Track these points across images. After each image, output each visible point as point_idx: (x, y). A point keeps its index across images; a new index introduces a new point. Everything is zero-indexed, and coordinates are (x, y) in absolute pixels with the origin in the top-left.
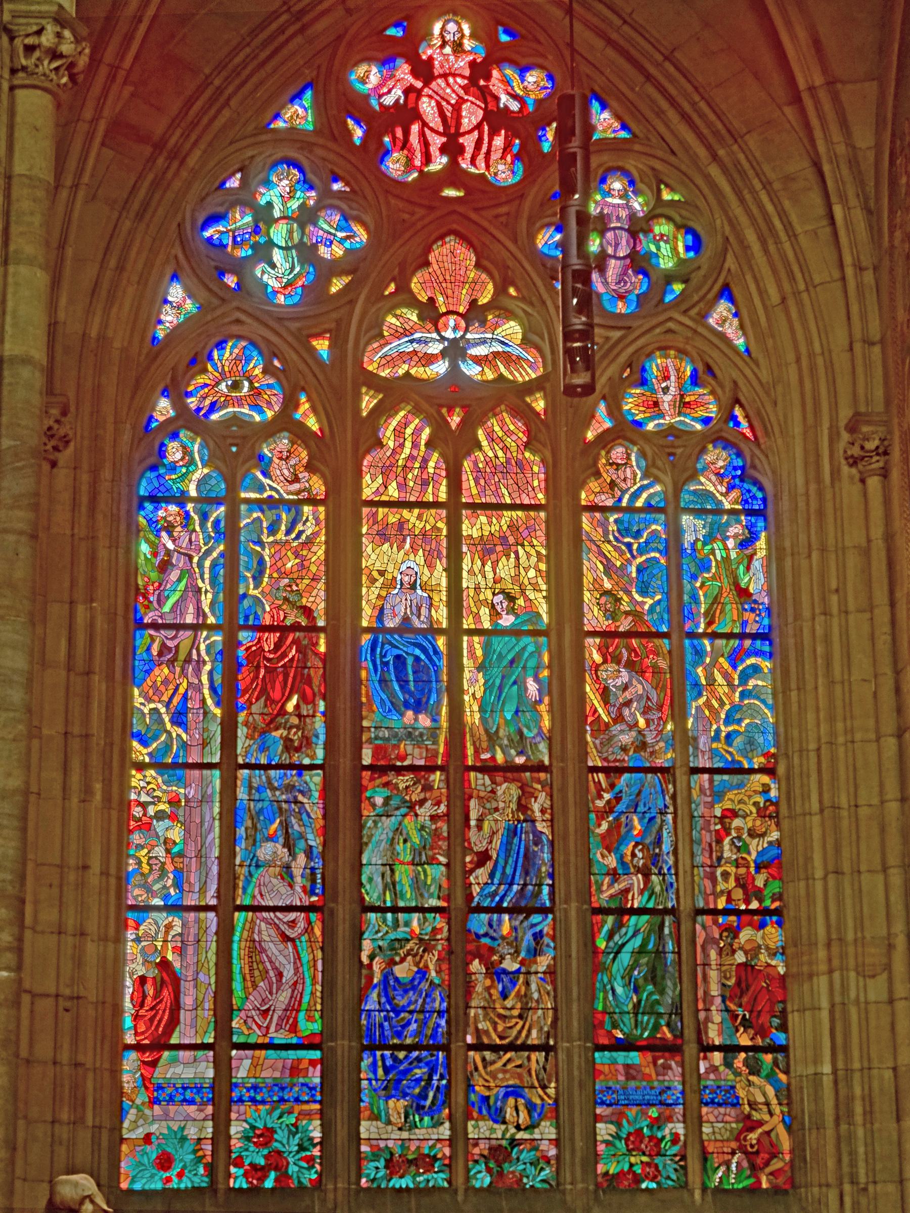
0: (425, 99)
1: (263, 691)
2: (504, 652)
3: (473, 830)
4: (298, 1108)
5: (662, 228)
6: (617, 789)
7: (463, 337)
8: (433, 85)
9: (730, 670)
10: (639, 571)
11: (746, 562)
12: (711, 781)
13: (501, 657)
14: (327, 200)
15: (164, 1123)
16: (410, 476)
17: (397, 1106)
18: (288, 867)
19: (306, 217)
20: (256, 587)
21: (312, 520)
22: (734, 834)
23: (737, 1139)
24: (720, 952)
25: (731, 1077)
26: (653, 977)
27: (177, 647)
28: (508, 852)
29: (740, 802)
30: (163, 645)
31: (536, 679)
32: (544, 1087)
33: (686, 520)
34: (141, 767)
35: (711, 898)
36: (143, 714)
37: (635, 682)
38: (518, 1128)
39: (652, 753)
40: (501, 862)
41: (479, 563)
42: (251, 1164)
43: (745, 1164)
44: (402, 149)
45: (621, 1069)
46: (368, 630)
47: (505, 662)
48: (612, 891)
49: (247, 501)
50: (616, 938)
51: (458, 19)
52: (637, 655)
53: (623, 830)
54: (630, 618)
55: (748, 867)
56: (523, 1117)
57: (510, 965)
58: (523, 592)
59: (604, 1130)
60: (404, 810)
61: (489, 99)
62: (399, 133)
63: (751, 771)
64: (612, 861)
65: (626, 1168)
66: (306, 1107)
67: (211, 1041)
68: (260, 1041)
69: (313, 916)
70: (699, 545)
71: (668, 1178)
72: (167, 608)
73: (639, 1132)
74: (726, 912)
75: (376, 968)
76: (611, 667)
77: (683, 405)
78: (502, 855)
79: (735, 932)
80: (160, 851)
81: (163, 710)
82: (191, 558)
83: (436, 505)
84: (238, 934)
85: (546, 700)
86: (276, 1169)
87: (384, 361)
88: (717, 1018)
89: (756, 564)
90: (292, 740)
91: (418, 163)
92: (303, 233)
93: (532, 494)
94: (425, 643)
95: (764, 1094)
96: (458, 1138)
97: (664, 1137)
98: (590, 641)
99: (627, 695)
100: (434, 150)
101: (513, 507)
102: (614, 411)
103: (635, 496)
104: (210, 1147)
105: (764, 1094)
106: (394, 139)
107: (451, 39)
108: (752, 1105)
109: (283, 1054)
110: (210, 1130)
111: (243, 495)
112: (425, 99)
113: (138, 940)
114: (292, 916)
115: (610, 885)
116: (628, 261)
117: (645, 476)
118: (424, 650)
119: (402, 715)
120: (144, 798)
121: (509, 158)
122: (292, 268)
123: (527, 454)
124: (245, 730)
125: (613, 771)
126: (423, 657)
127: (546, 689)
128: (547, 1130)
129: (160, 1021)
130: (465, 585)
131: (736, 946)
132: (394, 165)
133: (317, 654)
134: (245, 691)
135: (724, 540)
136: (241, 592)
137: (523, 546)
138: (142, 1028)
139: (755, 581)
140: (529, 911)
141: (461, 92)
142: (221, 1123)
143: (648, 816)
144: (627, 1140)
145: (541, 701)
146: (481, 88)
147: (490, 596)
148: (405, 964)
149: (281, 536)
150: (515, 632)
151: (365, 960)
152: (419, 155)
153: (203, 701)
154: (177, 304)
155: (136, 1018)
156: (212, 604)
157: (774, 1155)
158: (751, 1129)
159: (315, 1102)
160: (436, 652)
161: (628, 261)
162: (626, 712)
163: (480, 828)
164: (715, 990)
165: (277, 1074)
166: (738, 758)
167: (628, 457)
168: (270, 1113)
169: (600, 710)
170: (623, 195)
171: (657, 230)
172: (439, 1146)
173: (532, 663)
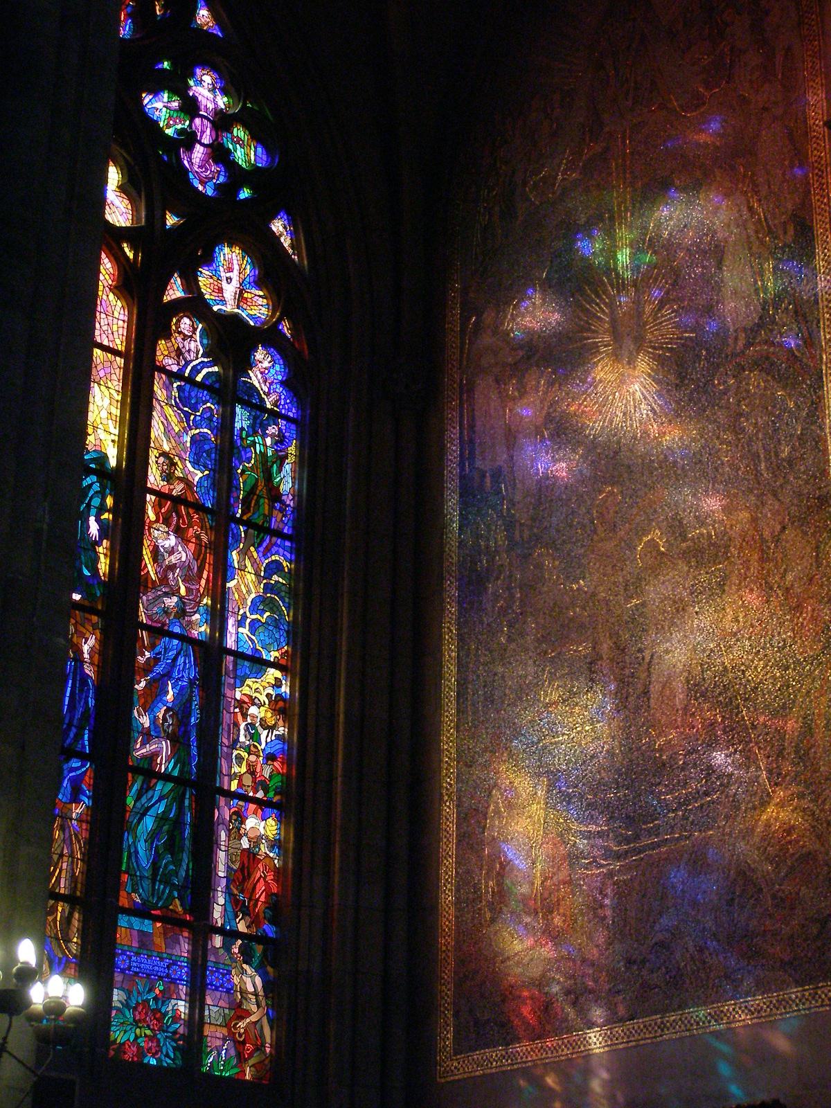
6: (158, 649)
11: (279, 462)
12: (235, 664)
23: (227, 1026)
24: (229, 836)
25: (228, 962)
26: (172, 846)
29: (256, 690)
31: (98, 520)
35: (226, 778)
43: (233, 1052)
45: (135, 933)
48: (144, 751)
50: (144, 800)
54: (182, 486)
55: (258, 756)
64: (145, 721)
70: (244, 433)
71: (167, 1056)
76: (163, 528)
77: (240, 298)
95: (254, 985)
98: (148, 497)
99: (173, 559)
103: (196, 371)
108: (243, 992)
115: (143, 744)
123: (111, 296)
127: (104, 530)
131: (242, 831)
135: (264, 436)
137: (99, 384)
139: (286, 481)
144: (135, 1009)
145: (99, 543)
158: (241, 1018)
167: (195, 330)
169: (149, 566)
170: (213, 90)
173: (96, 502)
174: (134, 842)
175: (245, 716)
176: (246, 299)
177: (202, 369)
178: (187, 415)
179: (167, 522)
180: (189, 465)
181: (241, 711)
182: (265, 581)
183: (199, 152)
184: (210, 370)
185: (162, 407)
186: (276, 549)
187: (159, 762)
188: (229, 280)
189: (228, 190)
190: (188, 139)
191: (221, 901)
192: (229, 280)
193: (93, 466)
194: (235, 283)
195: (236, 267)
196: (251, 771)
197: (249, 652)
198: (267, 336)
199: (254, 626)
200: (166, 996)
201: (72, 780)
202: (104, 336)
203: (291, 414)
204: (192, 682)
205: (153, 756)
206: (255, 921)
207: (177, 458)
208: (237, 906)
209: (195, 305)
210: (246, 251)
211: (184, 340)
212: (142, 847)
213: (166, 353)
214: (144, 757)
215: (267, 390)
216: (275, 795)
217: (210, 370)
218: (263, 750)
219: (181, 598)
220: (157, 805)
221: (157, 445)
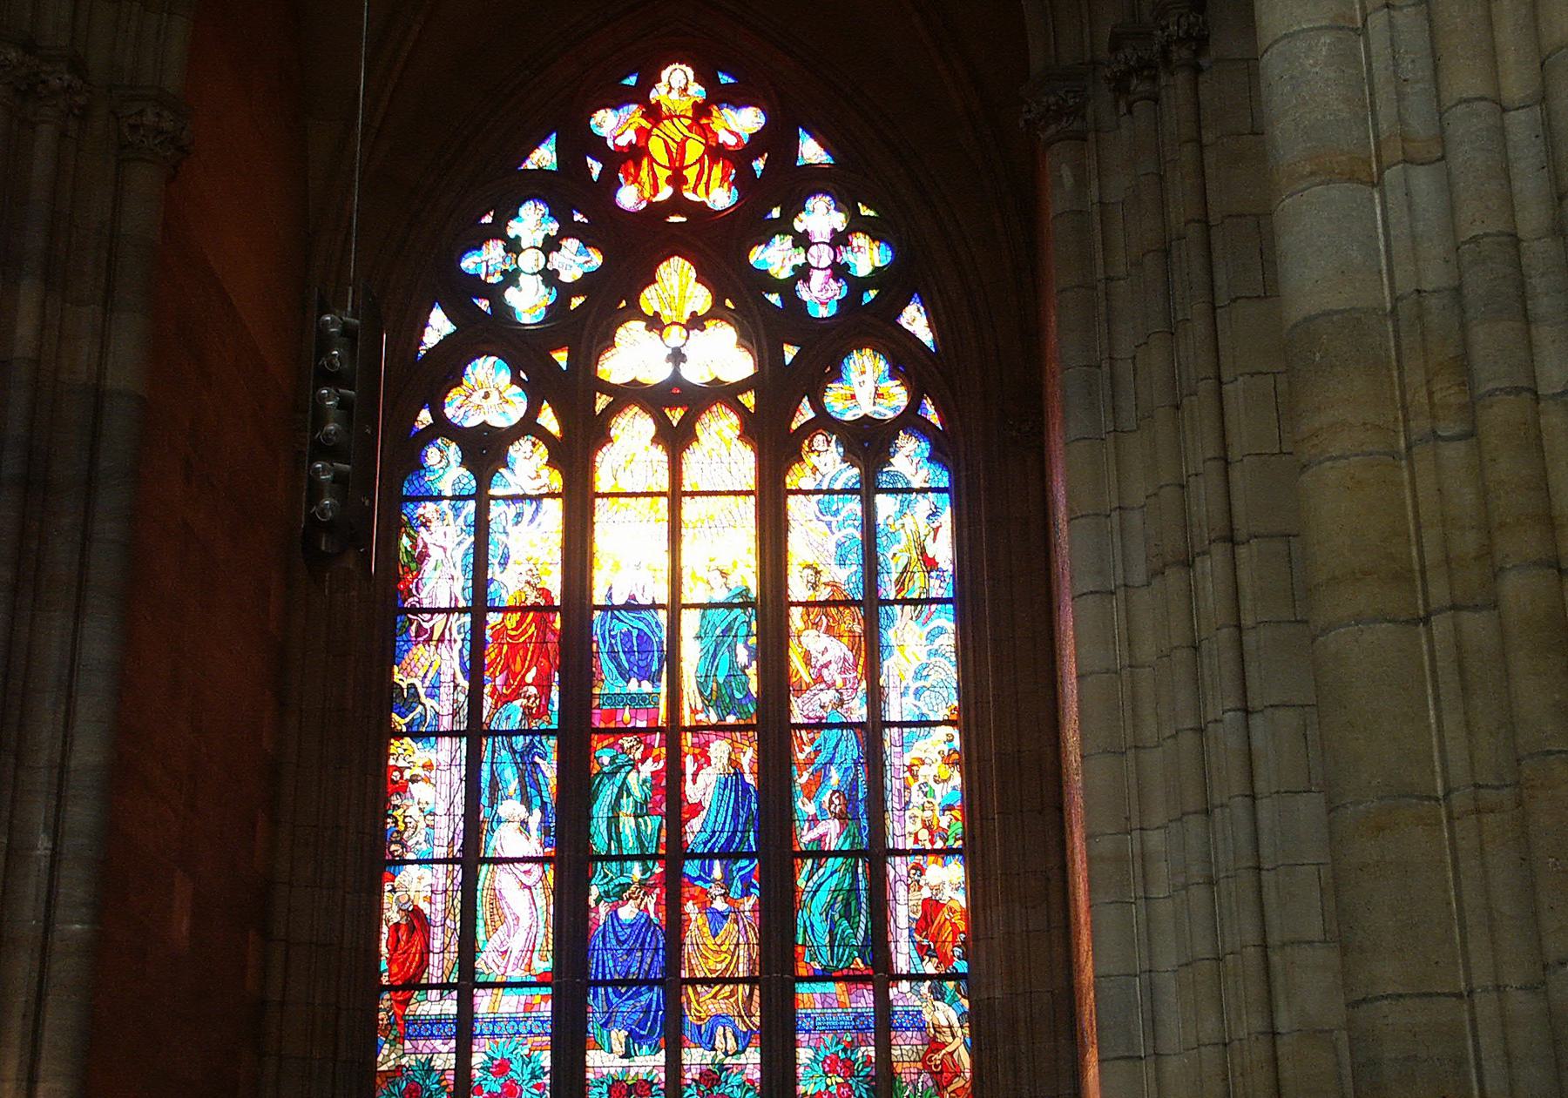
1: (506, 667)
10: (838, 546)
14: (568, 229)
18: (524, 823)
19: (550, 245)
21: (554, 510)
22: (921, 780)
23: (923, 1060)
26: (847, 915)
27: (432, 628)
31: (746, 646)
32: (749, 1017)
33: (880, 499)
34: (400, 736)
38: (726, 1054)
43: (930, 1083)
47: (718, 632)
50: (815, 878)
51: (683, 67)
56: (731, 1043)
57: (720, 905)
58: (735, 565)
59: (804, 1055)
60: (628, 768)
64: (811, 809)
69: (547, 867)
72: (423, 595)
73: (836, 1054)
74: (915, 852)
75: (603, 909)
76: (813, 632)
78: (714, 806)
79: (920, 869)
81: (419, 685)
91: (647, 195)
94: (649, 618)
96: (674, 1066)
100: (661, 182)
101: (729, 493)
102: (818, 405)
103: (834, 479)
108: (937, 1028)
109: (519, 990)
113: (393, 890)
114: (527, 866)
115: (810, 829)
118: (648, 625)
120: (401, 763)
128: (753, 1056)
132: (628, 197)
133: (554, 631)
134: (490, 665)
138: (395, 969)
139: (943, 551)
140: (739, 856)
141: (686, 132)
142: (463, 1054)
146: (702, 126)
150: (729, 606)
151: (593, 904)
152: (647, 186)
154: (439, 326)
155: (390, 961)
157: (958, 1073)
158: (938, 1051)
162: (825, 672)
163: (694, 782)
164: (903, 922)
166: (925, 711)
167: (829, 442)
171: (855, 242)
173: (743, 630)
175: (915, 777)
178: (829, 524)
179: (816, 625)
183: (818, 278)
188: (866, 387)
189: (849, 305)
190: (803, 273)
192: (866, 387)
195: (869, 367)
196: (927, 826)
198: (909, 421)
199: (917, 692)
200: (851, 1046)
201: (742, 879)
204: (856, 763)
205: (821, 838)
206: (944, 959)
208: (922, 951)
209: (824, 422)
210: (876, 350)
212: (816, 920)
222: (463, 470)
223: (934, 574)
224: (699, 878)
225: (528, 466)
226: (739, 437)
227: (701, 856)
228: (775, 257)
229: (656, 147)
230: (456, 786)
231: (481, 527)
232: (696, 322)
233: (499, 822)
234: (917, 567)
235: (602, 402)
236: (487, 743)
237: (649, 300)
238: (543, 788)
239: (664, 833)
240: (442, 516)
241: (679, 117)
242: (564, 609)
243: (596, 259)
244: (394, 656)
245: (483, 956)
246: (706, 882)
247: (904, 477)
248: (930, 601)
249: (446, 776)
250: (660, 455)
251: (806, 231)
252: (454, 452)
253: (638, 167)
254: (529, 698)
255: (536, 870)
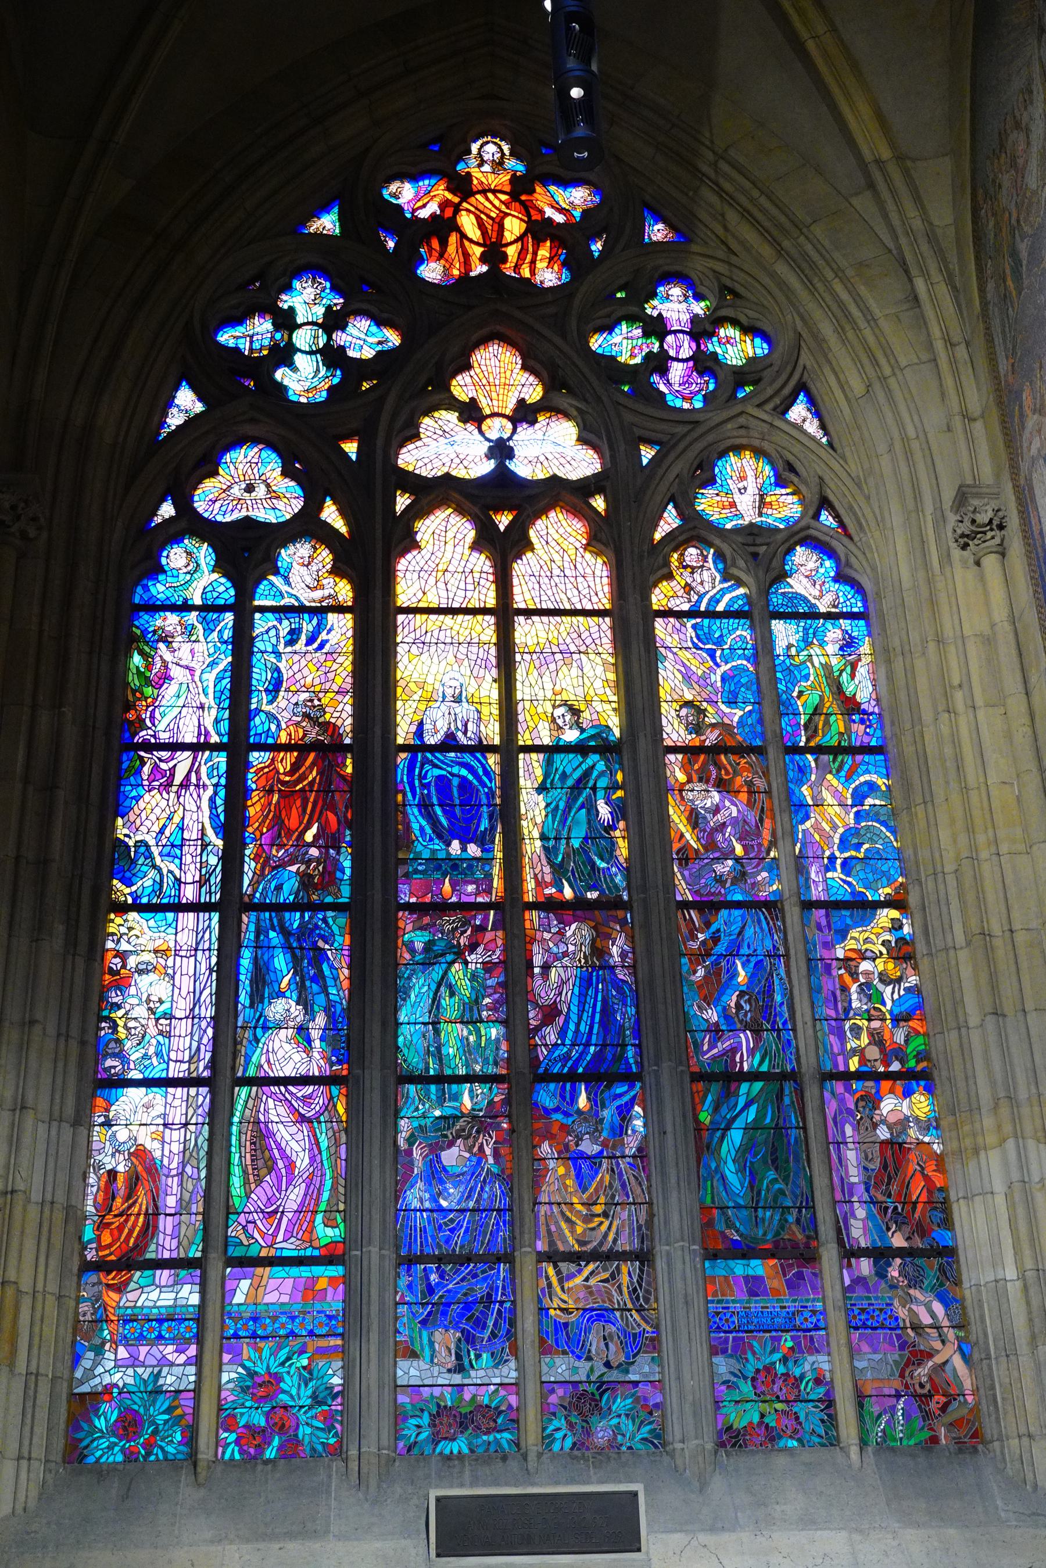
0: (463, 213)
2: (568, 771)
3: (538, 981)
4: (313, 1344)
5: (728, 331)
7: (510, 438)
8: (472, 200)
9: (840, 788)
13: (564, 776)
15: (130, 1371)
16: (452, 581)
17: (445, 1339)
18: (302, 1030)
19: (333, 322)
20: (271, 702)
21: (341, 629)
24: (857, 1127)
28: (582, 1004)
29: (866, 941)
30: (156, 767)
34: (122, 909)
36: (128, 847)
37: (727, 803)
38: (608, 1364)
39: (754, 885)
40: (574, 1018)
41: (536, 673)
42: (247, 1426)
44: (439, 259)
46: (404, 748)
47: (570, 782)
49: (263, 610)
50: (724, 1110)
51: (497, 140)
52: (727, 773)
53: (724, 978)
54: (717, 732)
55: (884, 1020)
58: (588, 702)
60: (449, 958)
61: (532, 212)
62: (435, 244)
63: (878, 905)
64: (712, 1015)
65: (756, 1419)
66: (322, 1343)
67: (199, 1255)
68: (263, 1254)
69: (335, 1090)
70: (793, 651)
72: (161, 727)
73: (769, 1369)
74: (859, 1076)
75: (416, 1153)
76: (699, 786)
77: (762, 503)
78: (574, 1009)
79: (873, 1101)
80: (141, 1012)
81: (152, 843)
82: (192, 670)
83: (484, 611)
84: (238, 1114)
85: (622, 824)
86: (282, 1429)
87: (420, 463)
88: (861, 1213)
89: (862, 671)
90: (312, 877)
92: (330, 338)
93: (595, 599)
94: (474, 763)
97: (802, 1376)
98: (671, 757)
100: (475, 260)
104: (191, 1403)
105: (933, 1315)
106: (431, 249)
107: (489, 160)
109: (295, 1271)
110: (192, 1379)
111: (256, 603)
112: (463, 213)
116: (691, 364)
117: (725, 580)
119: (449, 844)
120: (124, 946)
121: (556, 267)
122: (318, 370)
123: (588, 555)
124: (253, 864)
125: (708, 906)
126: (470, 777)
127: (619, 810)
129: (131, 1232)
130: (519, 697)
131: (877, 1118)
133: (343, 777)
136: (253, 706)
137: (586, 653)
141: (503, 208)
143: (753, 960)
144: (753, 1379)
147: (550, 710)
148: (454, 1150)
149: (300, 646)
150: (580, 749)
151: (401, 1142)
153: (203, 829)
156: (217, 721)
159: (336, 1335)
160: (486, 773)
161: (691, 364)
162: (720, 838)
165: (285, 1299)
167: (705, 559)
168: (275, 1354)
169: (688, 836)
171: (722, 332)
172: (502, 1392)
173: (603, 783)
174: (718, 1166)
175: (854, 975)
176: (770, 503)
177: (722, 596)
178: (712, 654)
180: (723, 707)
181: (851, 975)
182: (855, 809)
183: (677, 371)
184: (734, 594)
185: (675, 654)
186: (864, 768)
187: (738, 1059)
190: (659, 363)
191: (861, 1213)
193: (593, 743)
194: (752, 489)
195: (750, 474)
196: (876, 1038)
197: (848, 898)
202: (585, 601)
203: (856, 610)
207: (705, 704)
209: (696, 530)
211: (692, 573)
212: (730, 1170)
213: (671, 594)
214: (714, 1058)
215: (817, 593)
216: (917, 1062)
217: (734, 594)
218: (891, 1012)
219: (737, 860)
220: (745, 1114)
221: (676, 697)
222: (216, 576)
223: (856, 717)
224: (557, 1110)
225: (304, 573)
226: (586, 547)
227: (558, 1078)
228: (623, 344)
229: (468, 223)
230: (203, 978)
231: (242, 644)
232: (524, 414)
233: (265, 1028)
234: (831, 705)
235: (402, 502)
236: (248, 921)
237: (462, 387)
238: (330, 982)
239: (504, 1046)
240: (188, 631)
241: (494, 192)
242: (361, 747)
243: (394, 339)
244: (118, 805)
245: (242, 1219)
246: (567, 1114)
247: (805, 600)
248: (852, 751)
249: (188, 965)
250: (481, 563)
251: (660, 314)
252: (205, 554)
253: (444, 244)
254: (308, 863)
255: (319, 1096)
